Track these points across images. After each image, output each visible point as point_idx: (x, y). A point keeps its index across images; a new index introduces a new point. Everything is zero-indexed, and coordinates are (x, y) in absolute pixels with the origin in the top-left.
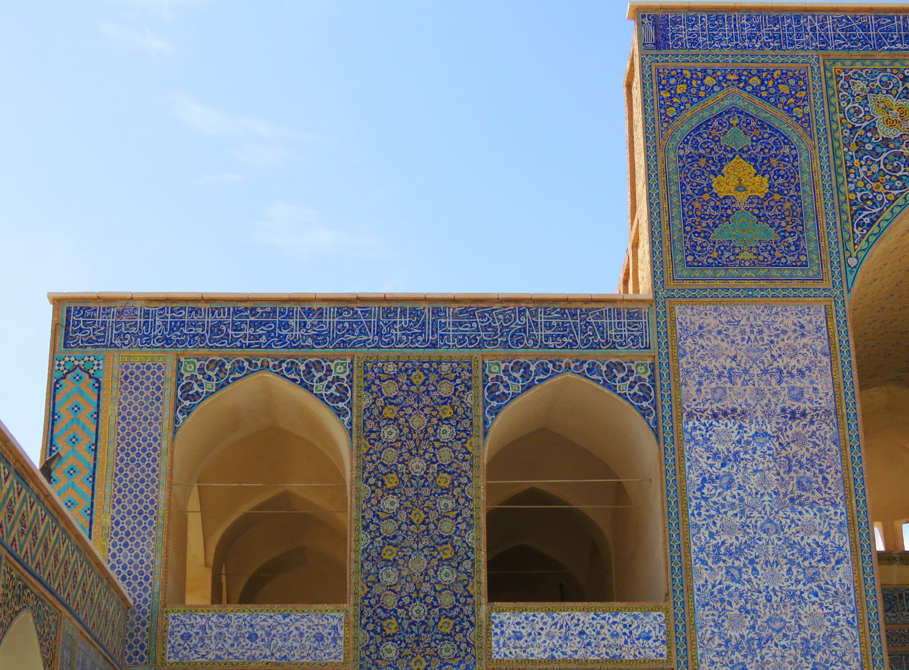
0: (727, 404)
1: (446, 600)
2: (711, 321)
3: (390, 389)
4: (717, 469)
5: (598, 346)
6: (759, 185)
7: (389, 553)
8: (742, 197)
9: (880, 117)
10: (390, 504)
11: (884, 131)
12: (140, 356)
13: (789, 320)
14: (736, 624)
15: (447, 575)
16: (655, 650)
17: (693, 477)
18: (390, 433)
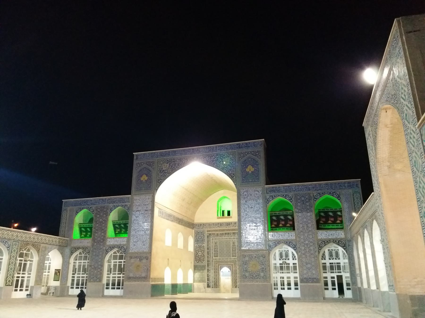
0: (138, 210)
1: (102, 237)
2: (138, 198)
3: (99, 210)
4: (136, 218)
5: (123, 203)
6: (146, 178)
7: (97, 232)
8: (144, 180)
9: (163, 167)
10: (97, 225)
11: (164, 169)
12: (71, 207)
13: (147, 197)
14: (135, 239)
15: (103, 234)
16: (125, 243)
17: (133, 220)
18: (98, 216)
